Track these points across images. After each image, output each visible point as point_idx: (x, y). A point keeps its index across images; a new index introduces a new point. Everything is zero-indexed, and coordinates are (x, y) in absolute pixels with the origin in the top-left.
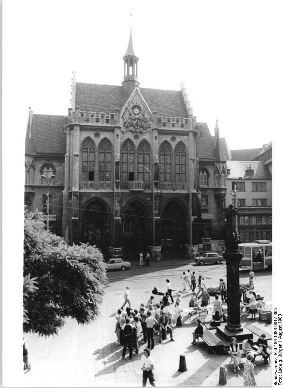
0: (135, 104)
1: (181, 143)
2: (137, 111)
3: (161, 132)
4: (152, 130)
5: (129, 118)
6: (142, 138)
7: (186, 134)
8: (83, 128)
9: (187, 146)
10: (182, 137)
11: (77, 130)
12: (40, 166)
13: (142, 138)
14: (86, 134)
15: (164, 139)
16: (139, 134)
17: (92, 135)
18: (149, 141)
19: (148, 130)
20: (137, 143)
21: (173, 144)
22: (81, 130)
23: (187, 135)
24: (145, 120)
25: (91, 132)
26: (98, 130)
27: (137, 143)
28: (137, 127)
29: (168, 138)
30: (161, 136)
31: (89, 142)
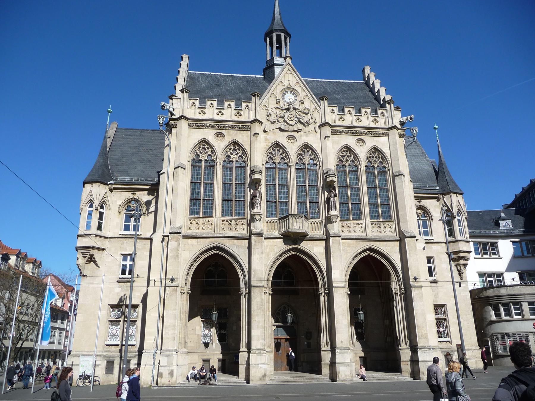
0: (286, 84)
1: (375, 149)
2: (289, 97)
3: (336, 130)
4: (321, 126)
5: (277, 108)
6: (301, 139)
7: (384, 132)
8: (194, 123)
9: (389, 156)
10: (376, 139)
11: (183, 125)
12: (120, 202)
13: (301, 139)
14: (199, 134)
15: (343, 143)
16: (295, 134)
17: (210, 135)
18: (316, 146)
19: (311, 127)
20: (293, 149)
21: (362, 152)
22: (191, 126)
23: (387, 135)
24: (307, 111)
25: (206, 131)
26: (220, 126)
27: (293, 149)
28: (291, 123)
29: (351, 141)
30: (336, 137)
31: (204, 149)
